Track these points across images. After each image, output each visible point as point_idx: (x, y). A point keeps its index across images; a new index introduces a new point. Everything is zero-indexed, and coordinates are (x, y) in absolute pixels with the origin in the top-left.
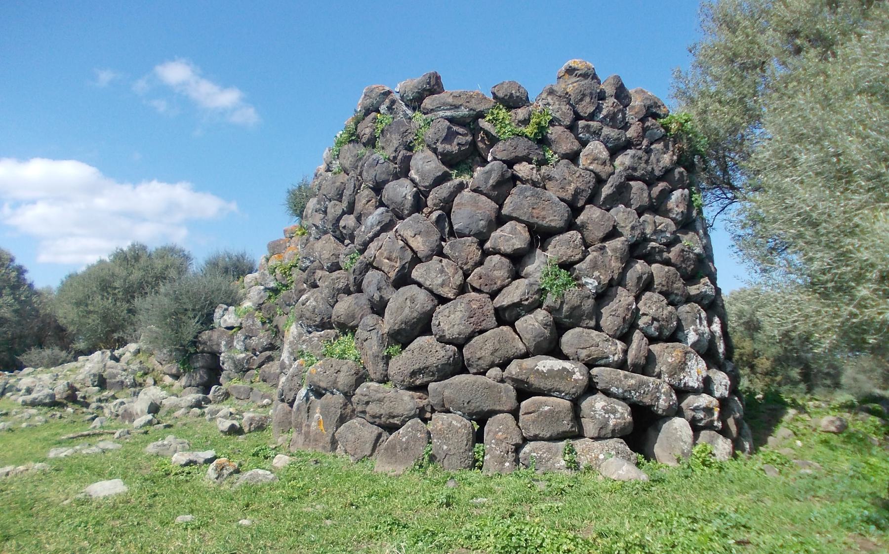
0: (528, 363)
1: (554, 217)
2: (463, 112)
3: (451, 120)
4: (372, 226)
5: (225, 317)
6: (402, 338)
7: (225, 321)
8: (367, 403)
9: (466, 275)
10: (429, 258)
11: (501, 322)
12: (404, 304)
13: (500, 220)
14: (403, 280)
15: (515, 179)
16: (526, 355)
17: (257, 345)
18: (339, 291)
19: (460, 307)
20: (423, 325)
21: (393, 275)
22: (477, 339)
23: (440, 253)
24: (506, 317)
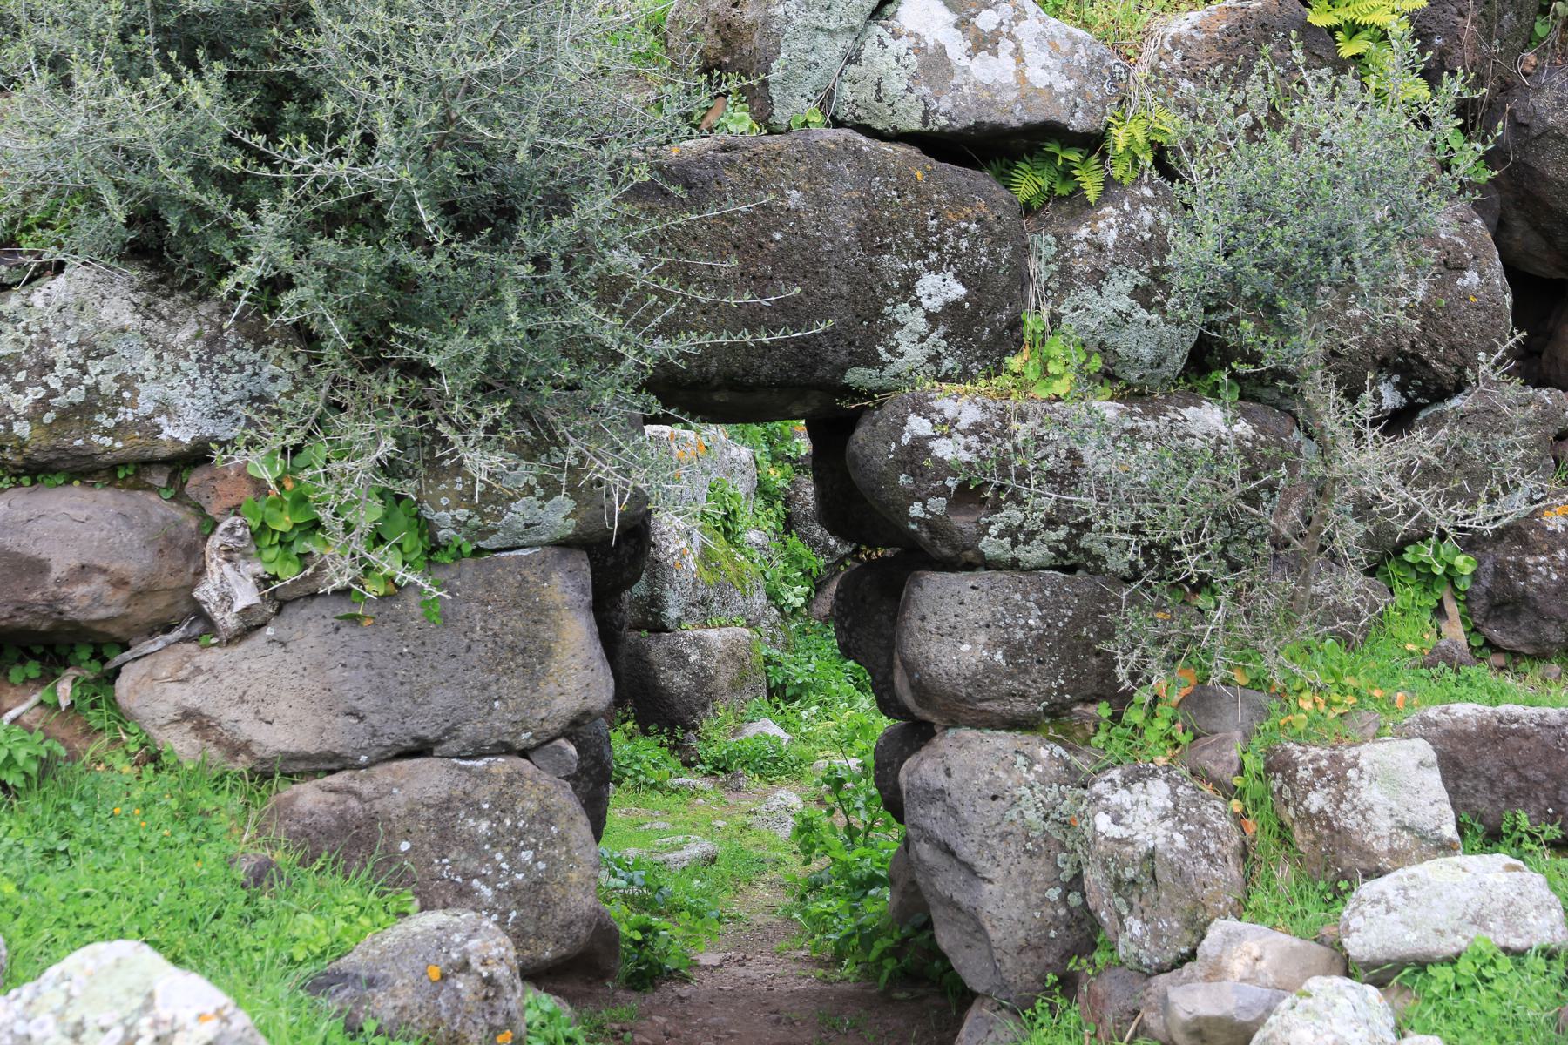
7: (934, 64)
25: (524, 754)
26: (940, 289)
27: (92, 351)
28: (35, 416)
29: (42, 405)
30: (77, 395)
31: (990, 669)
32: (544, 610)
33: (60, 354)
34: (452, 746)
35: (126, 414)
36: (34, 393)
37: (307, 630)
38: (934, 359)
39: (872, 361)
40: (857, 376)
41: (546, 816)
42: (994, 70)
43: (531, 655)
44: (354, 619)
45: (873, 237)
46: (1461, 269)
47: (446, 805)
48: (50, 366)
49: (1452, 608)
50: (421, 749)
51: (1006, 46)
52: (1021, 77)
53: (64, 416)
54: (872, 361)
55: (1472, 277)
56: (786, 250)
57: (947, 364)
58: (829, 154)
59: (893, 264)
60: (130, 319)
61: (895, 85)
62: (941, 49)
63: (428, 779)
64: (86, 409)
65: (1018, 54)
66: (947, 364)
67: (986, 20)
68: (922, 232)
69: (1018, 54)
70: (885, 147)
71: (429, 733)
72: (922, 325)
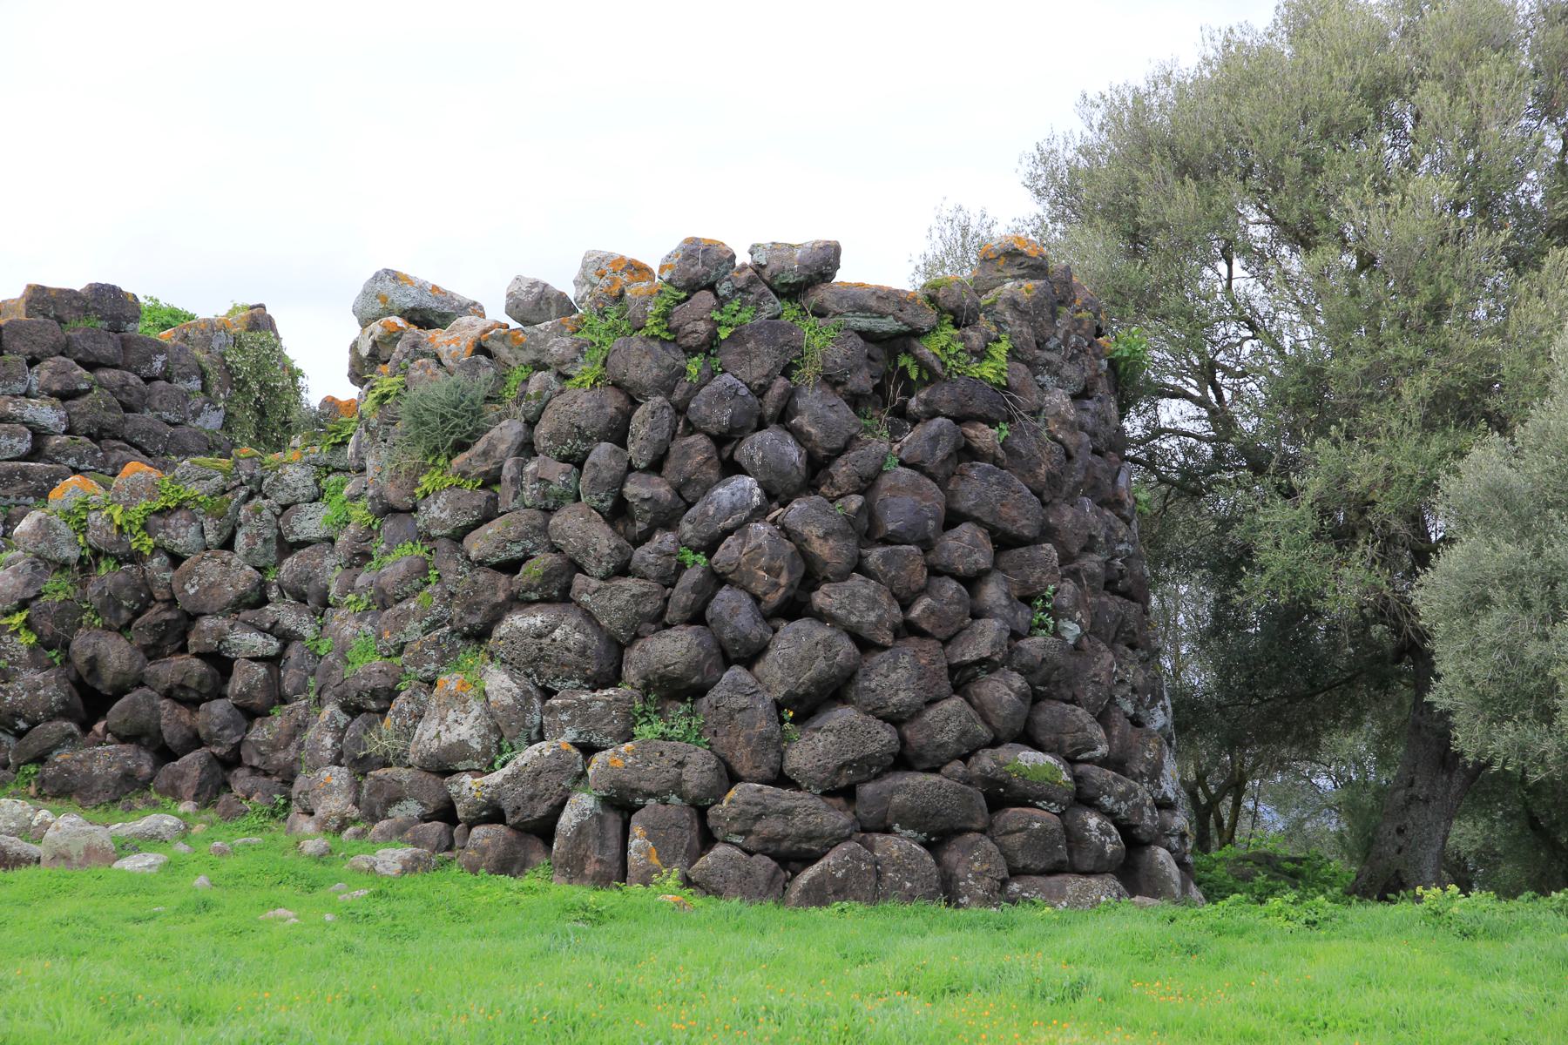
0: (1003, 753)
1: (1021, 516)
2: (888, 325)
3: (866, 335)
4: (733, 509)
6: (803, 708)
8: (758, 817)
9: (906, 606)
10: (843, 577)
11: (959, 688)
12: (797, 652)
13: (952, 519)
14: (794, 608)
15: (967, 452)
16: (995, 743)
17: (26, 704)
18: (644, 617)
19: (905, 661)
20: (834, 690)
21: (774, 598)
22: (930, 714)
23: (859, 567)
24: (962, 678)
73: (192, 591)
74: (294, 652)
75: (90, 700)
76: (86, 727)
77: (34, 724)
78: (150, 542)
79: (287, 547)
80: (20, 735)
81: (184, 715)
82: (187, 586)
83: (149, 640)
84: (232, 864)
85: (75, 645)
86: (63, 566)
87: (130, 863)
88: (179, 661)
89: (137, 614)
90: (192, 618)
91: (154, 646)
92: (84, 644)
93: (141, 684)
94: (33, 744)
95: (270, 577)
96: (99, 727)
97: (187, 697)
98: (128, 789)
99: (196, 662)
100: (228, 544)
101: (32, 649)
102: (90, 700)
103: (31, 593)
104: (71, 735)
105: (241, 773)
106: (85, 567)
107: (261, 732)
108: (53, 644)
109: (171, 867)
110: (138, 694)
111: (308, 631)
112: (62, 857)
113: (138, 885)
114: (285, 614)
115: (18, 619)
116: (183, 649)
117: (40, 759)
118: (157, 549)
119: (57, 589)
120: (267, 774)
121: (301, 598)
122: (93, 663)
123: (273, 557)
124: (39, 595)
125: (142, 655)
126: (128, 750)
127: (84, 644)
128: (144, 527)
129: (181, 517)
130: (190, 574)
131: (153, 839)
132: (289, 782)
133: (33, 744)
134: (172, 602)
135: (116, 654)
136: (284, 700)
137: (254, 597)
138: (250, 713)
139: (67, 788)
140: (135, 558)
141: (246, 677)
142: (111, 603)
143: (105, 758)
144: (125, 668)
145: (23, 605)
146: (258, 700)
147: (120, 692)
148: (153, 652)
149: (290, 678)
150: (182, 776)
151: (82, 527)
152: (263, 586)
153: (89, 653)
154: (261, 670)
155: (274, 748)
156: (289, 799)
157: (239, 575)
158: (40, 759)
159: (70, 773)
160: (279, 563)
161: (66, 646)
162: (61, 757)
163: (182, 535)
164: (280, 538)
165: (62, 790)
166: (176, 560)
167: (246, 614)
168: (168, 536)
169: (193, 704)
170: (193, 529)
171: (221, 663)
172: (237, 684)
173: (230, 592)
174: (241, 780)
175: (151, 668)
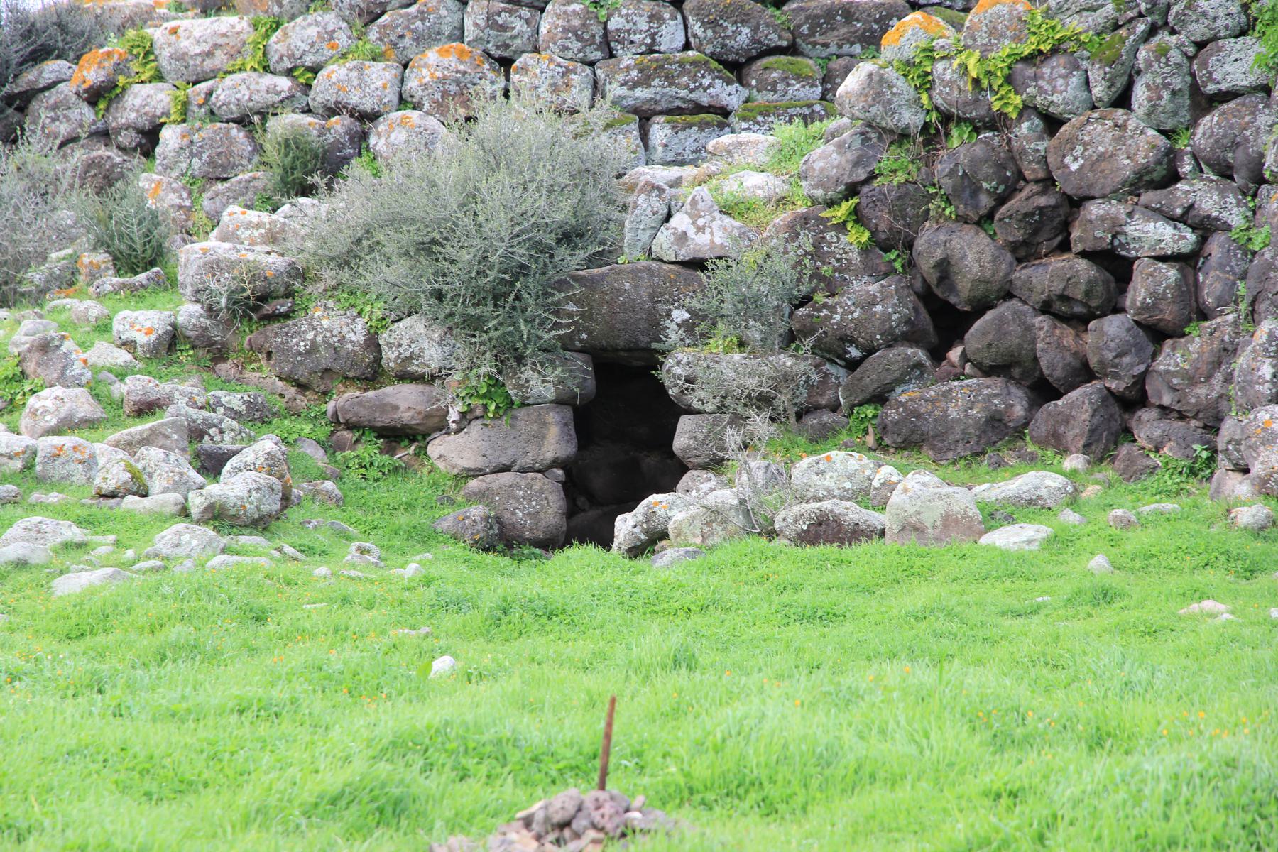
5: (680, 221)
7: (682, 238)
17: (859, 323)
25: (539, 471)
26: (680, 315)
27: (412, 341)
28: (395, 361)
29: (398, 357)
30: (407, 354)
31: (689, 446)
32: (545, 424)
33: (405, 342)
34: (516, 468)
35: (421, 360)
36: (396, 353)
37: (475, 428)
38: (682, 340)
39: (660, 340)
40: (655, 345)
41: (541, 491)
42: (703, 239)
43: (540, 438)
44: (486, 425)
45: (654, 298)
46: (875, 305)
47: (511, 486)
48: (400, 345)
49: (871, 430)
50: (506, 469)
51: (708, 230)
52: (712, 241)
53: (403, 361)
54: (660, 340)
55: (879, 308)
56: (624, 304)
57: (688, 341)
58: (640, 271)
59: (662, 307)
60: (423, 331)
61: (665, 246)
62: (685, 233)
63: (506, 478)
64: (411, 358)
65: (712, 234)
66: (688, 341)
67: (701, 222)
68: (672, 295)
69: (712, 234)
70: (665, 267)
71: (507, 463)
72: (675, 328)
73: (1074, 167)
74: (1216, 246)
75: (942, 319)
76: (938, 355)
77: (869, 351)
78: (1017, 100)
79: (1204, 102)
80: (852, 365)
81: (1067, 336)
82: (1068, 160)
83: (1018, 235)
84: (1138, 540)
85: (921, 244)
86: (903, 136)
87: (1005, 538)
88: (1058, 263)
89: (1002, 200)
90: (1075, 203)
91: (1025, 243)
92: (932, 243)
93: (1009, 295)
94: (871, 374)
95: (1180, 145)
96: (955, 354)
97: (1070, 313)
98: (996, 438)
99: (1083, 264)
100: (1123, 100)
101: (864, 250)
102: (942, 319)
103: (861, 175)
104: (919, 365)
105: (1146, 415)
106: (932, 136)
107: (1173, 359)
108: (892, 244)
109: (1059, 542)
110: (1005, 309)
111: (1236, 218)
112: (912, 528)
113: (1014, 567)
114: (1206, 197)
115: (843, 210)
116: (1065, 247)
117: (880, 398)
118: (1028, 109)
119: (895, 167)
120: (1182, 417)
121: (1225, 172)
122: (945, 268)
123: (1185, 116)
124: (872, 177)
125: (1009, 257)
126: (994, 385)
127: (932, 243)
128: (1009, 79)
129: (1058, 62)
130: (1072, 142)
131: (1032, 506)
132: (1212, 426)
133: (871, 374)
134: (1048, 182)
135: (975, 255)
136: (1204, 315)
137: (1159, 173)
138: (1158, 334)
139: (916, 437)
140: (997, 122)
141: (1150, 285)
142: (967, 185)
143: (964, 397)
144: (988, 274)
145: (852, 190)
146: (1168, 314)
147: (981, 307)
148: (1024, 252)
149: (1211, 284)
150: (1067, 420)
151: (926, 83)
152: (1171, 156)
153: (939, 254)
154: (1171, 273)
155: (1192, 380)
156: (1214, 452)
157: (1140, 143)
158: (880, 398)
159: (919, 416)
160: (1193, 124)
161: (909, 245)
162: (905, 395)
163: (1059, 88)
164: (1195, 89)
165: (909, 441)
166: (1052, 123)
167: (1149, 197)
168: (1041, 91)
169: (1080, 321)
170: (1075, 80)
171: (1115, 264)
172: (1138, 293)
173: (1126, 166)
174: (1147, 425)
175: (1021, 274)
